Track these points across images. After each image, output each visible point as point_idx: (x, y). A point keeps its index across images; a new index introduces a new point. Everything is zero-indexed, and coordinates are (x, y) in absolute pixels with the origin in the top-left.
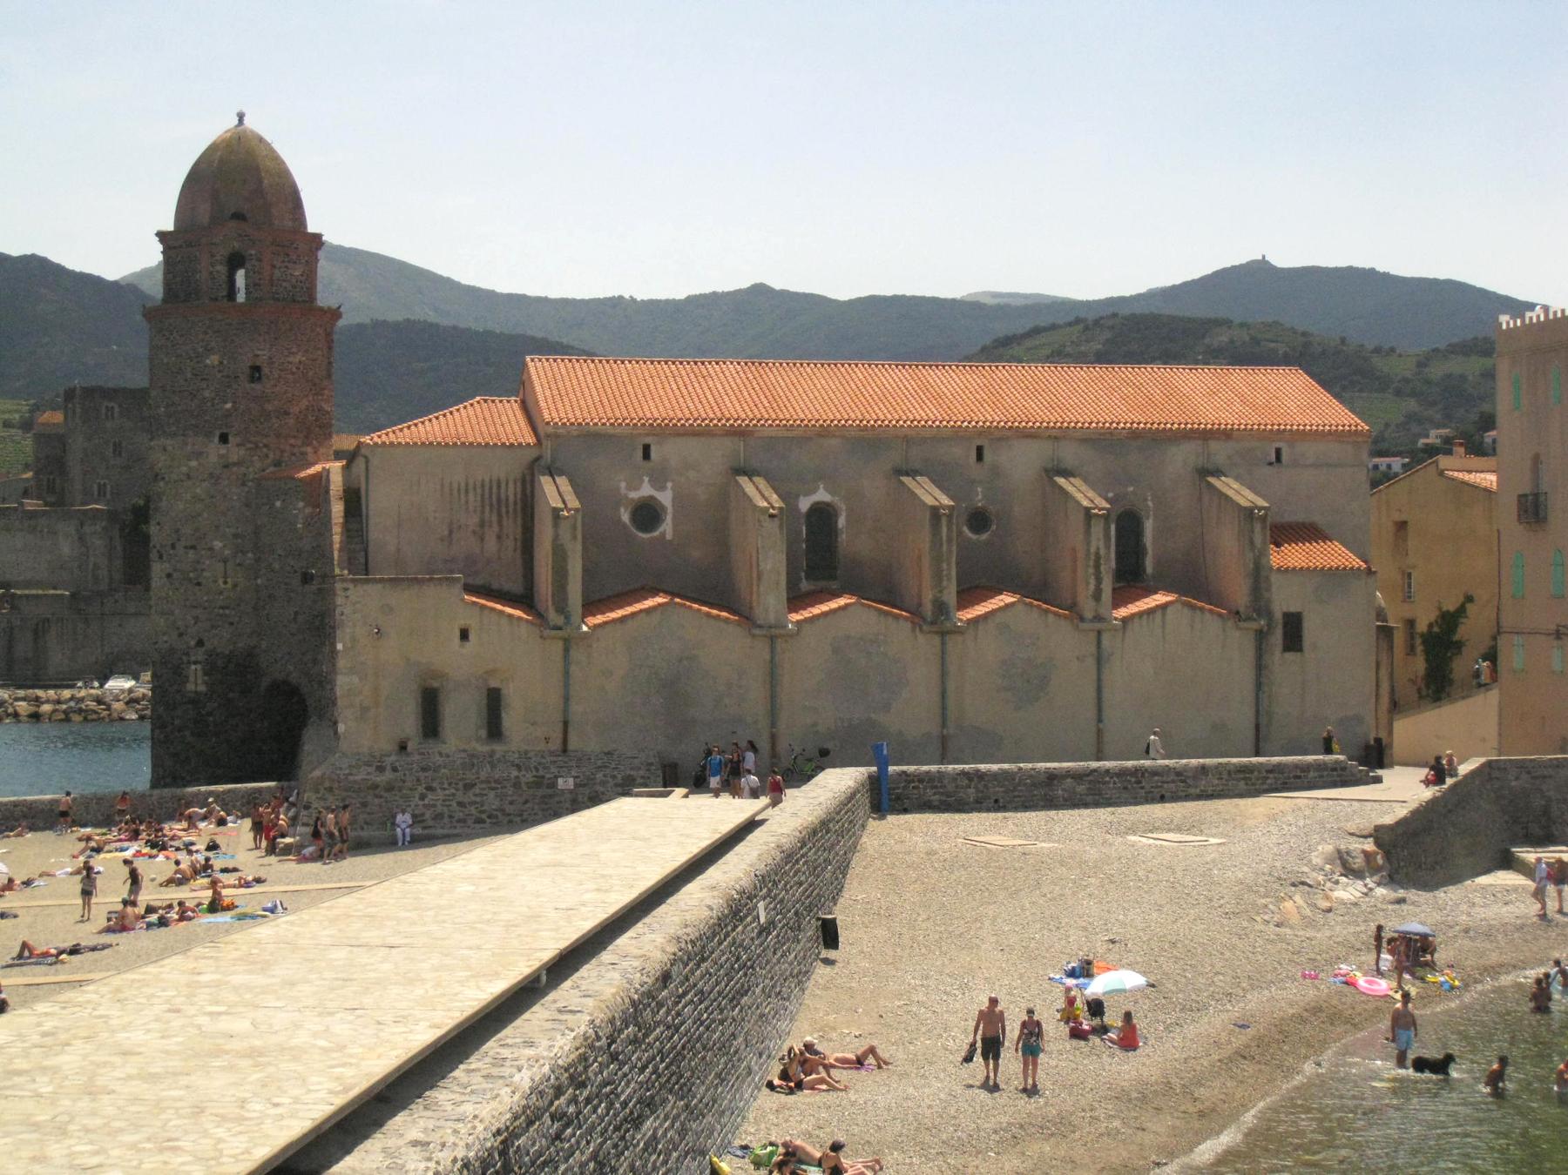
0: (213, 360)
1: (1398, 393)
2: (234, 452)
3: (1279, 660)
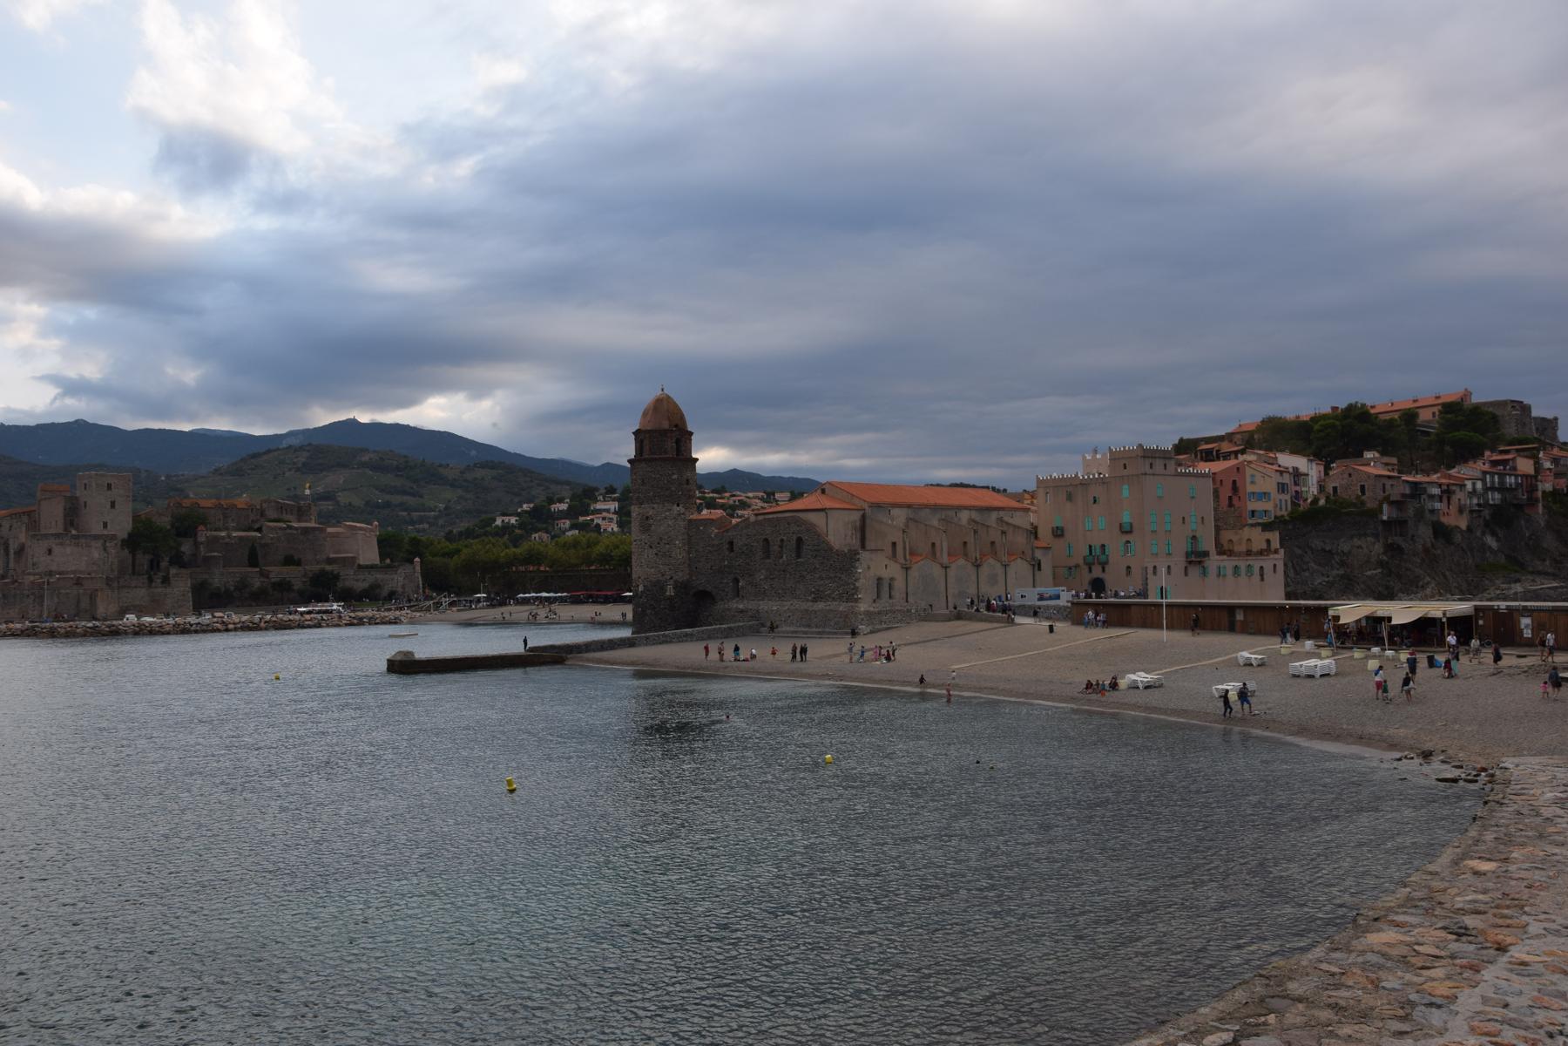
0: (675, 477)
1: (452, 485)
2: (681, 509)
3: (1037, 572)
